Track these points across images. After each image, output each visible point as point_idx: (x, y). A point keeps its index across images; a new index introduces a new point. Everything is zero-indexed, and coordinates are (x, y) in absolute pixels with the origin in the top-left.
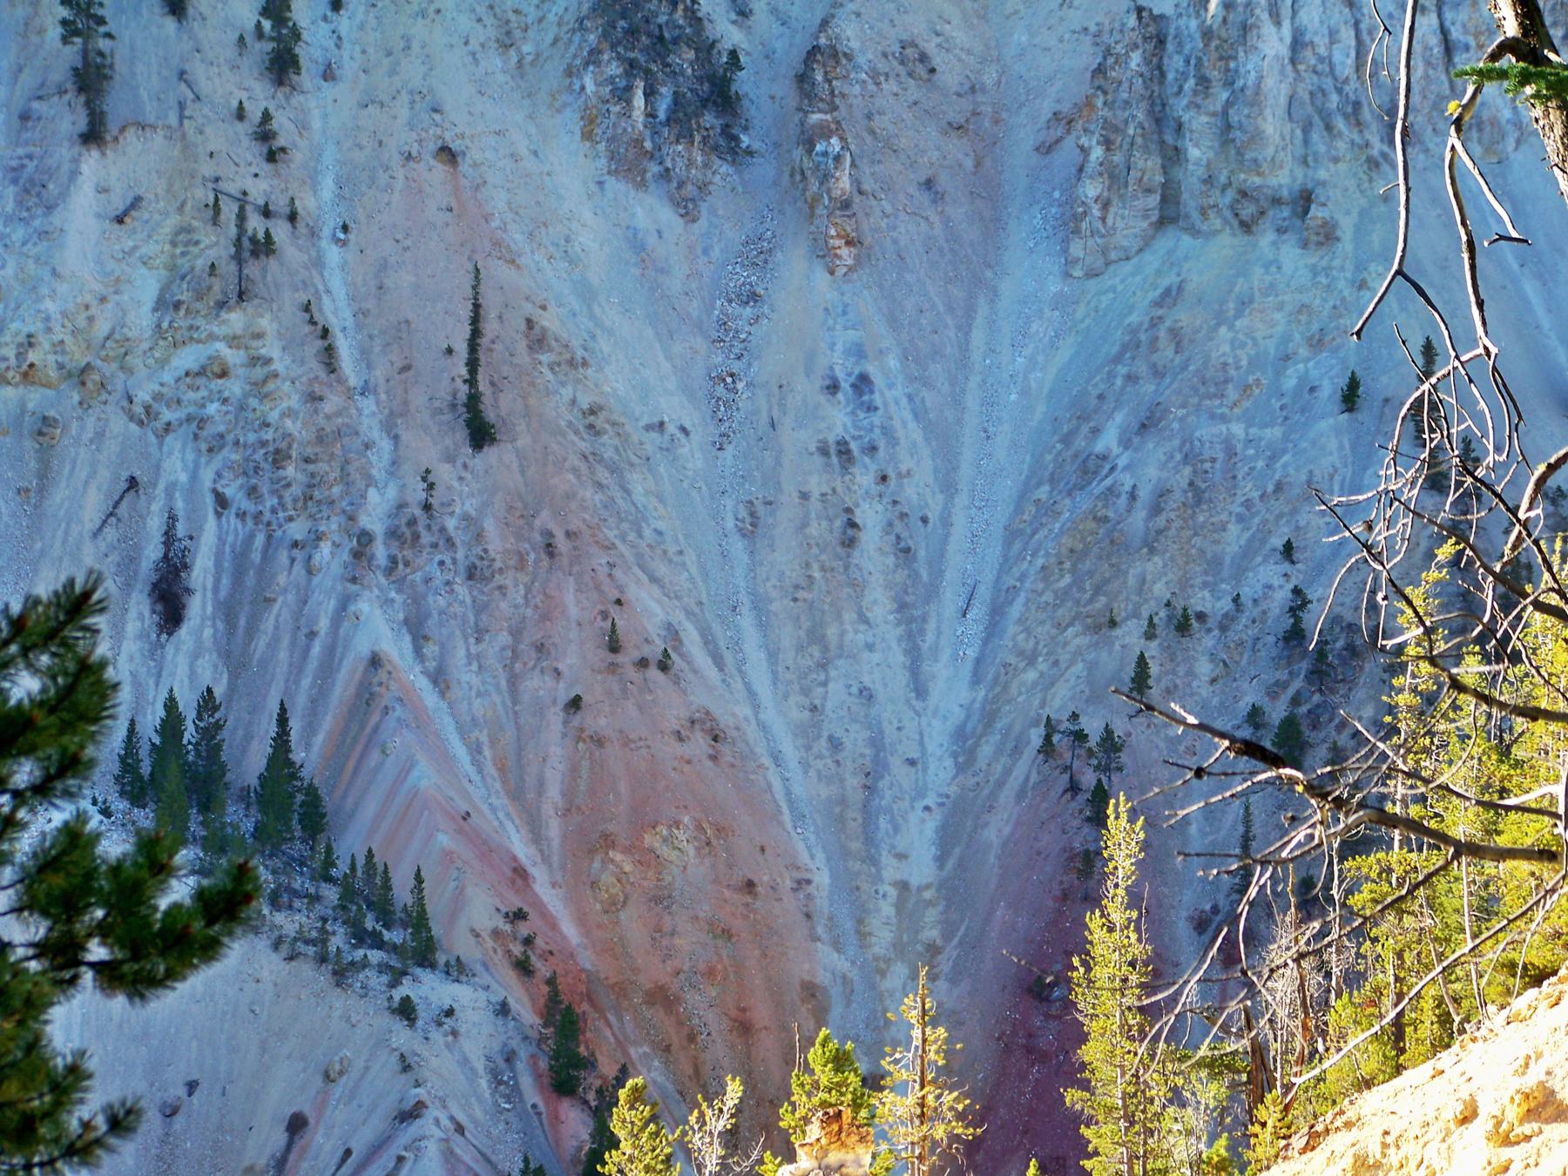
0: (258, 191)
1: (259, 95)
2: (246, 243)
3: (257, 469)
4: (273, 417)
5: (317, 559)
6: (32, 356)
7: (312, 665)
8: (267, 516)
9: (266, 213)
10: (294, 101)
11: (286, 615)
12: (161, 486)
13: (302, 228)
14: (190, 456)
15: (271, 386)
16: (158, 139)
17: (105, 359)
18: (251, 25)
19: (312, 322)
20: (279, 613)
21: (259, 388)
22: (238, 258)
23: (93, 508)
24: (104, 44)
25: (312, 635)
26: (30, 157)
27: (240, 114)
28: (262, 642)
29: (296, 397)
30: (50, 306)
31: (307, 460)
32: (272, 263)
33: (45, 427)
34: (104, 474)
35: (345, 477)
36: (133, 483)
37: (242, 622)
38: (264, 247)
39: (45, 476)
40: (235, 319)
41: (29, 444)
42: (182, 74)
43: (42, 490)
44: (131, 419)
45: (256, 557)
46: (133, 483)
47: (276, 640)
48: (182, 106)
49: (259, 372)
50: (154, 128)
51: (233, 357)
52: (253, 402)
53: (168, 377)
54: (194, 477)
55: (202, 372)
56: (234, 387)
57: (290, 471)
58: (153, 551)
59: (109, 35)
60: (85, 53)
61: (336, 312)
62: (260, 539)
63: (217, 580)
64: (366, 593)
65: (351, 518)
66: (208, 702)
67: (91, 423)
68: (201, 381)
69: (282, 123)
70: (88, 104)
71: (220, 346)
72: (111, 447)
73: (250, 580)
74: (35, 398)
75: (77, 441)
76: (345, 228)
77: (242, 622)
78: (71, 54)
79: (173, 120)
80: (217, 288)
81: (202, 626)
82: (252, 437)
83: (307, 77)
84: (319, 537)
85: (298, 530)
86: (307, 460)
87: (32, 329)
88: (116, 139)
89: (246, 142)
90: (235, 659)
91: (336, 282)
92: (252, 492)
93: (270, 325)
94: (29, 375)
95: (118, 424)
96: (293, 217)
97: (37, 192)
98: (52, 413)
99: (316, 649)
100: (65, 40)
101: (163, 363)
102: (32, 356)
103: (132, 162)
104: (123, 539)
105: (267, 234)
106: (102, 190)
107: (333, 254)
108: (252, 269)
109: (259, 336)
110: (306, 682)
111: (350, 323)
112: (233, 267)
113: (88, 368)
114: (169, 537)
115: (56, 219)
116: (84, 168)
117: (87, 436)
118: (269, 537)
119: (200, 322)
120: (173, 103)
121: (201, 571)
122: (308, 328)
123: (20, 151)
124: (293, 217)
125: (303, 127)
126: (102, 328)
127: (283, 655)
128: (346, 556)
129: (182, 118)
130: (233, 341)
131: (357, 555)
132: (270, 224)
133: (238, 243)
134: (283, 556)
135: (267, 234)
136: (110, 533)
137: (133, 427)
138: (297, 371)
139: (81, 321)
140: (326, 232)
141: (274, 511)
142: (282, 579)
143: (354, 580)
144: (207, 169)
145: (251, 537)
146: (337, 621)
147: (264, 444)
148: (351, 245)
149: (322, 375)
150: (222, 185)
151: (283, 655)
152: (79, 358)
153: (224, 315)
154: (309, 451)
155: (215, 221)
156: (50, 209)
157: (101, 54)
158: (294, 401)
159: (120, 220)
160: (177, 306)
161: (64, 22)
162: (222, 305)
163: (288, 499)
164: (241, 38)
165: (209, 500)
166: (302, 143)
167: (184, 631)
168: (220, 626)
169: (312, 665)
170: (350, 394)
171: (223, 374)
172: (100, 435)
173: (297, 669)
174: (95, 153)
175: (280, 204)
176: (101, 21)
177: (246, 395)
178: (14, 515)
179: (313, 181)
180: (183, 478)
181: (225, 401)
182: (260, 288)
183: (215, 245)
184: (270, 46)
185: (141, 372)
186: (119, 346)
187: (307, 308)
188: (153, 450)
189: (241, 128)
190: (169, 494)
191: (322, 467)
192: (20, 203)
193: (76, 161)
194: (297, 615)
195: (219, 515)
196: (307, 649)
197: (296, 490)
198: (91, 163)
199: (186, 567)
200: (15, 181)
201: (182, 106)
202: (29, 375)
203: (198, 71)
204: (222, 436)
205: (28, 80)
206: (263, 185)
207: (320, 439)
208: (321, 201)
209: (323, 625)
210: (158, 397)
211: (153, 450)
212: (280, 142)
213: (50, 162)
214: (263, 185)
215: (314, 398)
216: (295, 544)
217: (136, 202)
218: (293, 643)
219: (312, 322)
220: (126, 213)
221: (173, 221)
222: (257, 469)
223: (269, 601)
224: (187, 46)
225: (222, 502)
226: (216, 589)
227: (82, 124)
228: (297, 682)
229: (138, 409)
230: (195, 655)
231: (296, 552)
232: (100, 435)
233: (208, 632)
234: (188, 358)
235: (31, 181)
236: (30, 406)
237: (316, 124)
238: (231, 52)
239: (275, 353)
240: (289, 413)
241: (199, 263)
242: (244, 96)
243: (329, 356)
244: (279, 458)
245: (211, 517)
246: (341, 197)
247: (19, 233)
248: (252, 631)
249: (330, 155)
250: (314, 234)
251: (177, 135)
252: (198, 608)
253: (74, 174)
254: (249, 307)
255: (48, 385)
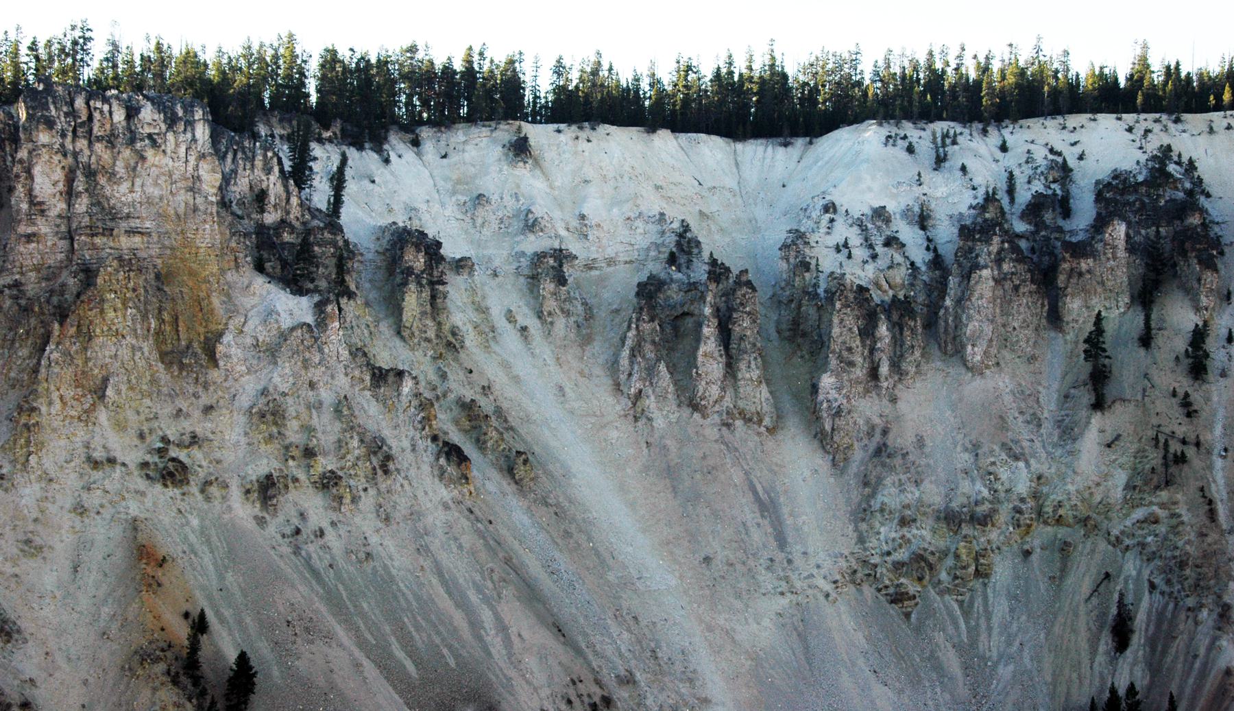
0: (1181, 431)
1: (1183, 383)
2: (1171, 456)
3: (1171, 570)
4: (1180, 544)
5: (1200, 617)
6: (1061, 512)
7: (1194, 673)
8: (1176, 594)
9: (1184, 442)
10: (1204, 387)
11: (1182, 644)
12: (1122, 577)
13: (1202, 450)
14: (1138, 562)
15: (1180, 528)
16: (1131, 407)
17: (1098, 513)
18: (1183, 350)
19: (1204, 496)
20: (1179, 643)
21: (1174, 529)
22: (1166, 465)
23: (1086, 586)
24: (1107, 361)
25: (1196, 656)
26: (1067, 415)
27: (1174, 394)
28: (1169, 659)
29: (1193, 534)
30: (1071, 488)
31: (1197, 566)
32: (1186, 467)
33: (1065, 549)
34: (1094, 571)
35: (1216, 575)
36: (1107, 575)
37: (1159, 648)
38: (1181, 459)
39: (1064, 570)
40: (1164, 495)
41: (1057, 555)
42: (1146, 376)
43: (1062, 578)
44: (1109, 543)
45: (1169, 616)
46: (1107, 575)
47: (1176, 657)
48: (1144, 390)
49: (1174, 521)
50: (1129, 401)
51: (1162, 513)
52: (1171, 536)
53: (1128, 523)
54: (1139, 573)
55: (1145, 521)
56: (1162, 529)
57: (1188, 572)
58: (1114, 610)
59: (1108, 357)
60: (1095, 367)
61: (1219, 491)
62: (1171, 606)
63: (1148, 625)
64: (1225, 637)
65: (1219, 597)
66: (1131, 689)
67: (1089, 545)
68: (1145, 525)
69: (1196, 397)
70: (1095, 390)
71: (1155, 508)
72: (1098, 557)
73: (1165, 627)
74: (1062, 532)
75: (1081, 554)
76: (1226, 450)
77: (1159, 648)
78: (1087, 368)
79: (1139, 397)
80: (1155, 480)
81: (1137, 651)
82: (1169, 554)
83: (1211, 376)
84: (1202, 606)
85: (1190, 602)
86: (1197, 566)
87: (1060, 498)
88: (1110, 407)
89: (1176, 407)
90: (1155, 667)
91: (1219, 477)
92: (1168, 582)
93: (1182, 500)
94: (1059, 521)
95: (1103, 545)
96: (1198, 444)
97: (1068, 432)
98: (1069, 540)
99: (1197, 665)
100: (1086, 359)
101: (1127, 515)
102: (1061, 512)
103: (1119, 418)
104: (1100, 604)
105: (1183, 453)
106: (1102, 431)
107: (1219, 463)
108: (1173, 469)
109: (1175, 503)
110: (1191, 681)
111: (1225, 496)
112: (1163, 469)
113: (1088, 518)
114: (1121, 604)
115: (1076, 446)
116: (1093, 421)
117: (1085, 552)
118: (1176, 605)
119: (1146, 496)
120: (1139, 388)
121: (1140, 619)
122: (1202, 500)
123: (1063, 413)
124: (1198, 444)
125: (1208, 400)
126: (1098, 498)
127: (1179, 666)
128: (1215, 616)
129: (1144, 396)
130: (1162, 506)
131: (1221, 616)
132: (1185, 448)
133: (1165, 457)
134: (1183, 616)
135: (1183, 453)
136: (1095, 601)
137: (1110, 547)
138: (1194, 521)
139: (1086, 495)
140: (1216, 451)
141: (1179, 592)
142: (1181, 627)
143: (1219, 629)
144: (1155, 421)
145: (1167, 604)
146: (1210, 648)
147: (1175, 557)
148: (1229, 459)
149: (1207, 522)
150: (1162, 429)
151: (1179, 666)
152: (1083, 511)
153: (1158, 493)
154: (1198, 562)
155: (1156, 446)
156: (1075, 440)
157: (1104, 366)
158: (1192, 536)
159: (1109, 446)
160: (1134, 488)
161: (1085, 351)
162: (1157, 487)
163: (1186, 586)
164: (1177, 358)
165: (1146, 584)
166: (1207, 408)
167: (1128, 652)
168: (1147, 649)
169: (1194, 673)
170: (1222, 533)
171: (1156, 522)
172: (1093, 551)
173: (1187, 673)
174: (1099, 414)
175: (1192, 437)
176: (1104, 350)
177: (1167, 533)
178: (1047, 590)
179: (1210, 427)
180: (1134, 573)
181: (1156, 535)
182: (1178, 480)
183: (1154, 458)
184: (1191, 361)
185: (1116, 521)
186: (1106, 508)
187: (1202, 489)
188: (1119, 559)
189: (1174, 400)
190: (1126, 581)
191: (1204, 570)
192: (1060, 437)
193: (1089, 418)
194: (1188, 646)
195: (1151, 593)
196: (1193, 663)
197: (1190, 581)
198: (1097, 420)
199: (1130, 619)
200: (1059, 427)
201: (1144, 390)
202: (1059, 521)
203: (1154, 372)
204: (1154, 553)
205: (1070, 379)
206: (1183, 429)
207: (1205, 555)
208: (1215, 435)
209: (1202, 651)
210: (1122, 532)
211: (1119, 559)
212: (1195, 407)
213: (1076, 418)
214: (1183, 429)
215: (1202, 535)
216: (1189, 609)
217: (1118, 437)
218: (1186, 660)
219: (1204, 496)
220: (1112, 442)
221: (1136, 446)
222: (1171, 570)
223: (1175, 638)
224: (1149, 361)
225: (1153, 586)
226: (1147, 630)
227: (1093, 400)
228: (1186, 681)
229: (1113, 539)
230: (1134, 664)
231: (1190, 613)
232: (1093, 551)
233: (1141, 653)
234: (1139, 514)
235: (1066, 427)
236: (1059, 536)
237: (1215, 399)
238: (1172, 364)
239: (1183, 513)
240: (1189, 542)
241: (1147, 466)
242: (1177, 385)
243: (1212, 514)
244: (1182, 565)
245: (1147, 593)
246: (1225, 434)
247: (1059, 452)
248: (1164, 652)
249: (1221, 413)
250: (1209, 453)
251: (1142, 405)
252: (1137, 640)
253: (1088, 423)
254: (1172, 489)
255: (1069, 526)
